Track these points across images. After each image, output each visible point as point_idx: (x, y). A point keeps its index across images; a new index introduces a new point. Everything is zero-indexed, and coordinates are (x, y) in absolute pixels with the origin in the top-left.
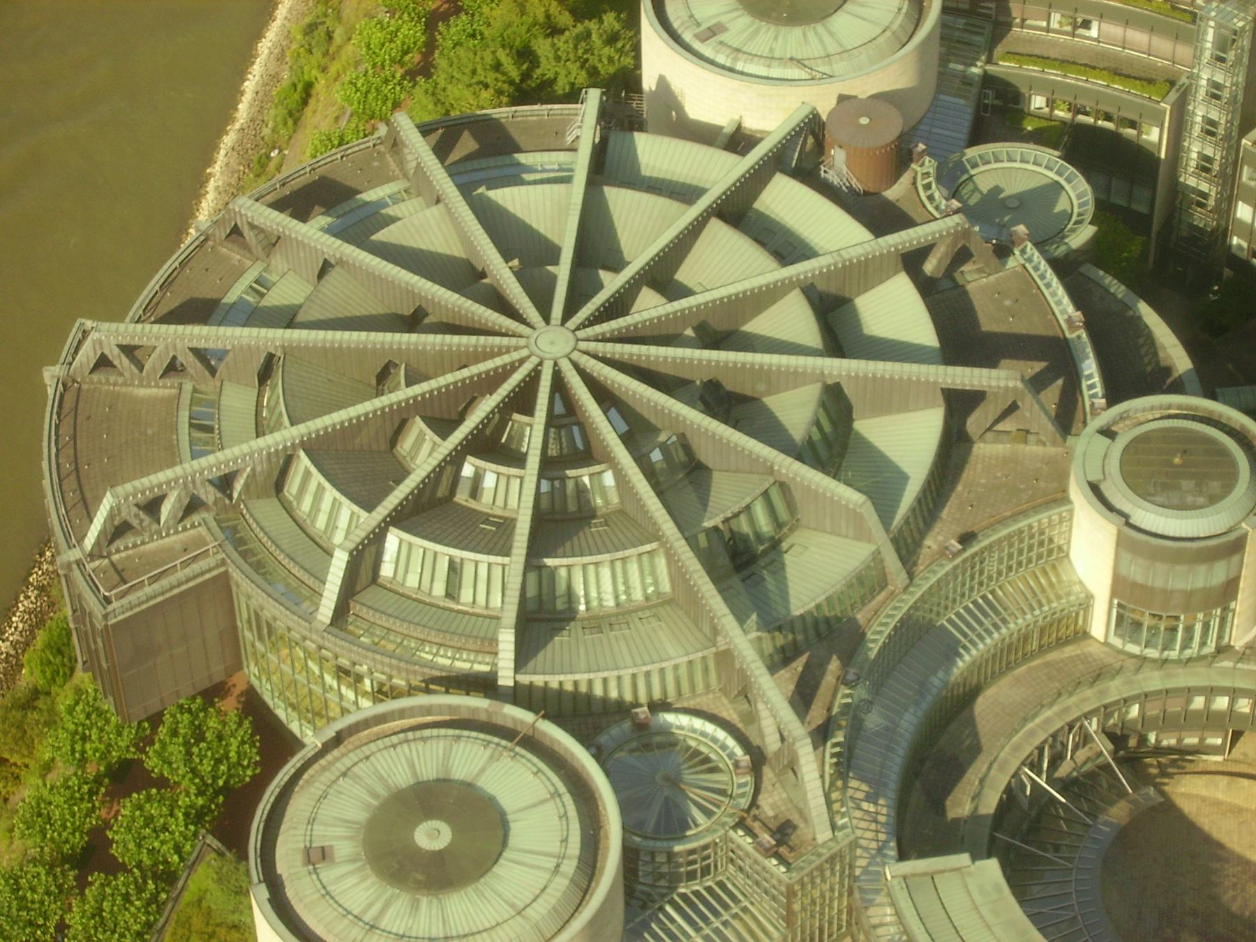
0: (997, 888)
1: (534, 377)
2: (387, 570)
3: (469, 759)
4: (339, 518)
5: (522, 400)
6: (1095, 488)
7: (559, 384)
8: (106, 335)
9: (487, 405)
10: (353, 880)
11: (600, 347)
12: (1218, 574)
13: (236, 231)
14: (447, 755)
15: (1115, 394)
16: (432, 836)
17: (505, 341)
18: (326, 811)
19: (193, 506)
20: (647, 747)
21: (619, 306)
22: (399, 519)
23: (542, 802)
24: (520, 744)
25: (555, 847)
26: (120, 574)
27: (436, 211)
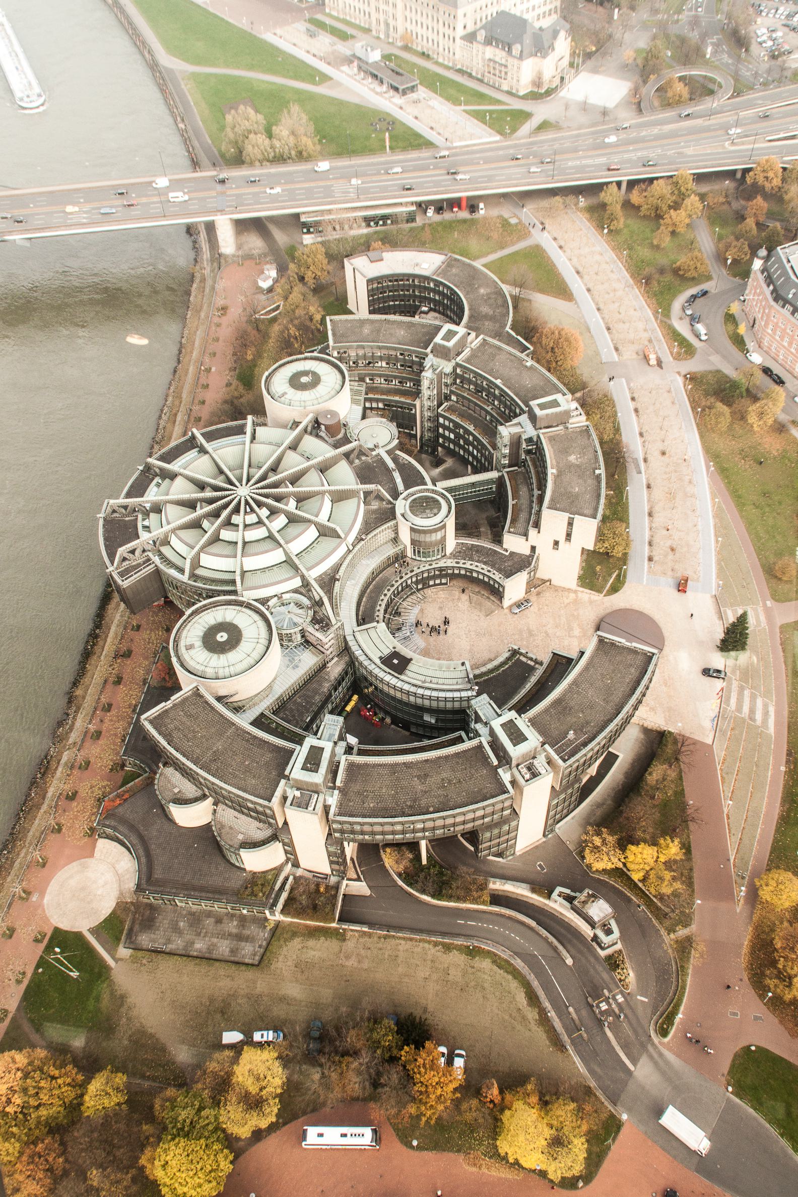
1: (239, 503)
5: (237, 510)
6: (403, 515)
7: (247, 503)
9: (225, 514)
11: (257, 491)
12: (439, 535)
15: (407, 487)
20: (283, 605)
21: (264, 478)
24: (246, 607)
27: (207, 456)
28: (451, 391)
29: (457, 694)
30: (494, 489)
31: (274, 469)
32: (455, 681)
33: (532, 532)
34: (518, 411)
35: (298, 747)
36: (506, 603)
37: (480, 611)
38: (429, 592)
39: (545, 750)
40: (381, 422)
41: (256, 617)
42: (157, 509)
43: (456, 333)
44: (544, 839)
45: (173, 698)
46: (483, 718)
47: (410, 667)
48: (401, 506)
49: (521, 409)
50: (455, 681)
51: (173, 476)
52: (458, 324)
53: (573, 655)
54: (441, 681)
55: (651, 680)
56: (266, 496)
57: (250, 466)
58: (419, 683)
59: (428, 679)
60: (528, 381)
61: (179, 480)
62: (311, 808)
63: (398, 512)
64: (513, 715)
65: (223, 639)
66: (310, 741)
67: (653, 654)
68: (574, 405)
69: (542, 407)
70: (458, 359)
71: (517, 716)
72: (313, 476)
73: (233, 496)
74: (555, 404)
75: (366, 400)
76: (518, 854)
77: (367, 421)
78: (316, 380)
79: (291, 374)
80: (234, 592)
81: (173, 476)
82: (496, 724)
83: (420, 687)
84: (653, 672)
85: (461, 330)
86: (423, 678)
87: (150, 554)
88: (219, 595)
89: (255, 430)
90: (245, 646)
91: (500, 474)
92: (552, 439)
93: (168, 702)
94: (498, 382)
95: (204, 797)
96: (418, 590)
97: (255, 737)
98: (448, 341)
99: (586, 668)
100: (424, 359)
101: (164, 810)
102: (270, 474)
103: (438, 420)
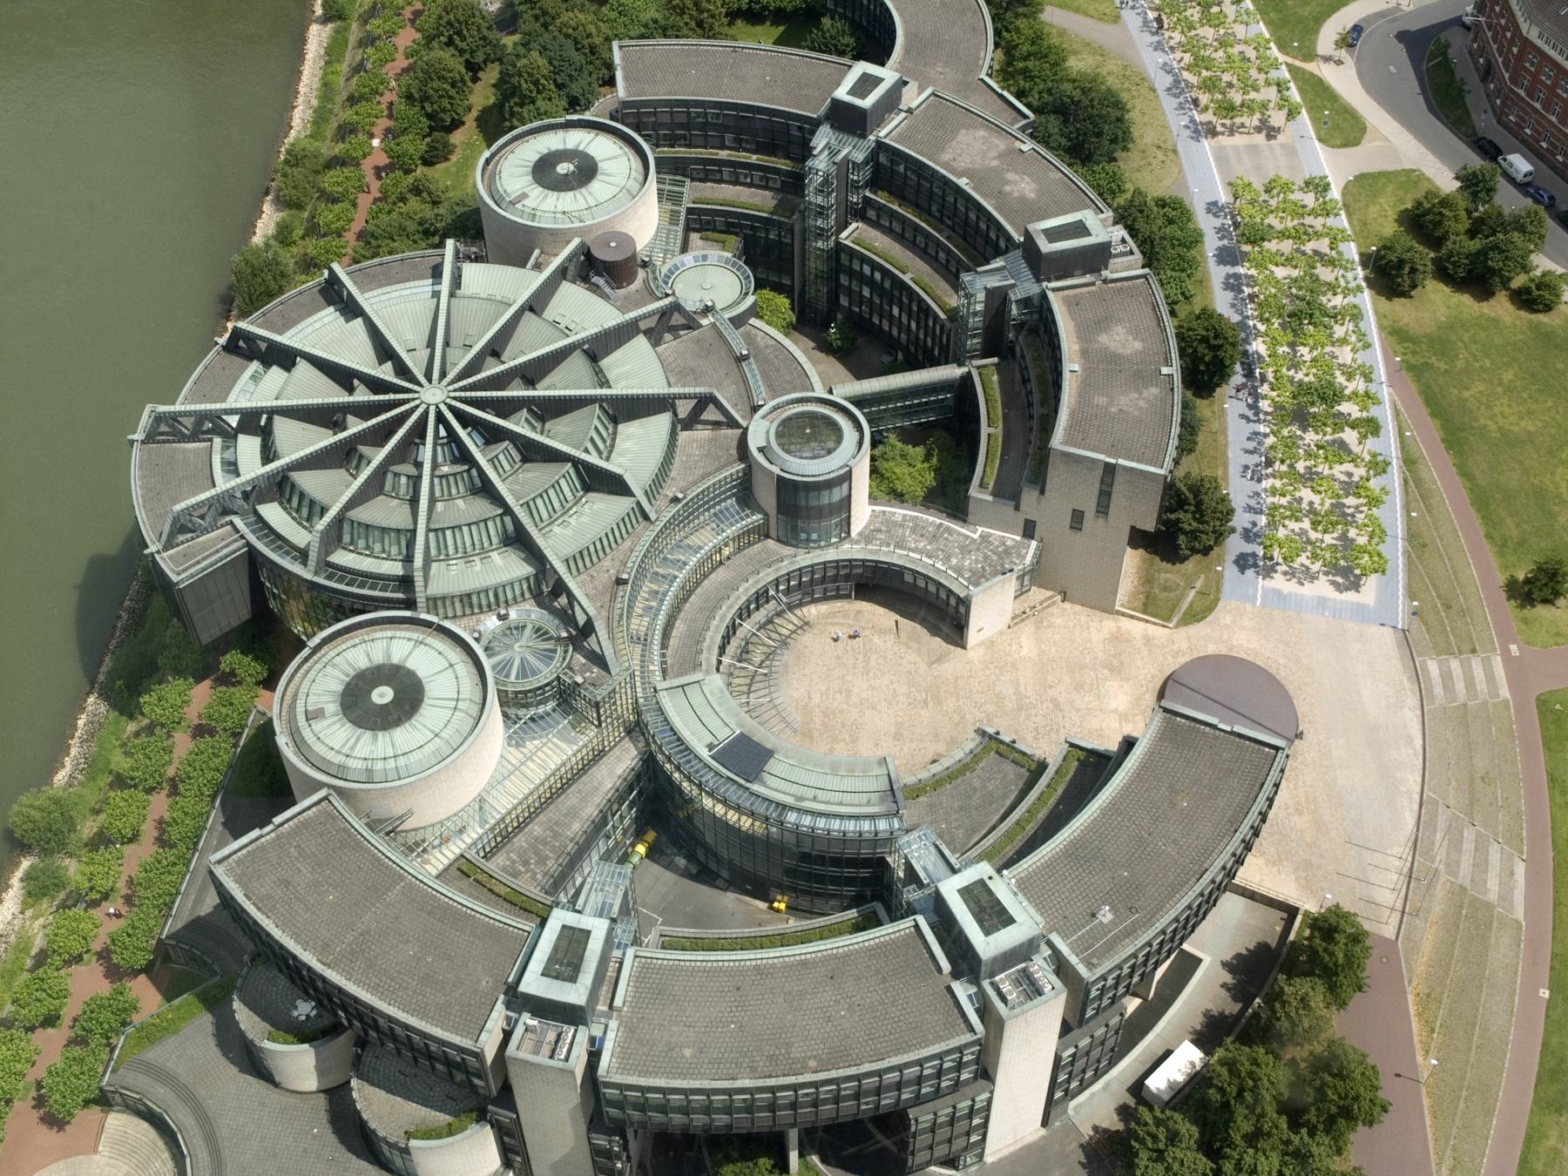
0: (721, 691)
1: (424, 418)
5: (419, 430)
6: (761, 450)
10: (337, 726)
12: (837, 494)
14: (388, 647)
17: (406, 396)
21: (473, 367)
27: (360, 320)
28: (866, 200)
29: (866, 826)
30: (951, 403)
31: (494, 350)
32: (864, 798)
33: (1029, 497)
34: (1002, 244)
36: (973, 636)
37: (919, 652)
38: (812, 611)
39: (1050, 944)
40: (720, 258)
41: (455, 654)
42: (256, 422)
43: (877, 81)
44: (1043, 1132)
45: (278, 820)
46: (922, 875)
47: (772, 766)
48: (760, 432)
49: (1009, 238)
50: (864, 798)
51: (285, 358)
52: (883, 64)
53: (1112, 745)
54: (837, 797)
55: (1271, 801)
56: (480, 404)
57: (447, 344)
58: (789, 800)
59: (810, 793)
60: (1023, 186)
61: (302, 367)
63: (754, 443)
64: (983, 870)
65: (386, 701)
66: (559, 918)
67: (1277, 749)
68: (1120, 232)
69: (1053, 235)
70: (882, 134)
71: (992, 872)
72: (577, 365)
73: (412, 404)
74: (1080, 229)
75: (690, 211)
76: (990, 1157)
77: (688, 259)
78: (587, 171)
79: (536, 157)
80: (410, 604)
81: (285, 358)
82: (951, 889)
83: (792, 808)
84: (1277, 785)
85: (887, 75)
86: (795, 789)
87: (237, 521)
88: (376, 609)
89: (459, 270)
90: (430, 715)
91: (964, 370)
92: (1073, 305)
93: (270, 827)
94: (963, 182)
95: (334, 1030)
96: (791, 608)
98: (863, 96)
99: (1138, 776)
100: (813, 133)
102: (490, 360)
103: (838, 259)
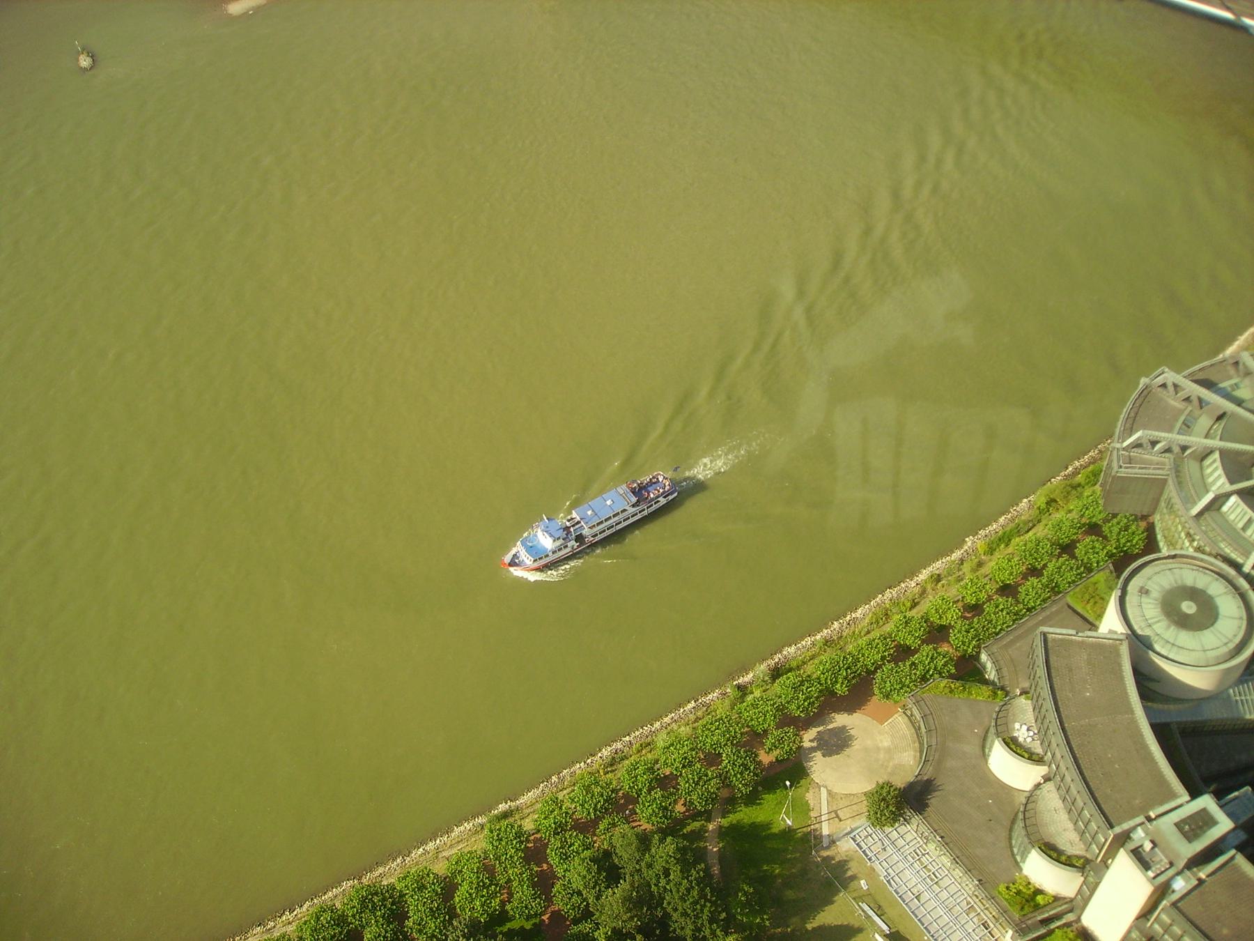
2: (1225, 509)
3: (1216, 589)
4: (1217, 479)
8: (1170, 376)
13: (1236, 363)
16: (1188, 607)
18: (1155, 578)
19: (1168, 450)
22: (1240, 493)
23: (1244, 529)
25: (1230, 636)
26: (1130, 460)
35: (1187, 798)
62: (1151, 874)
66: (1206, 802)
97: (1145, 747)
101: (985, 739)
